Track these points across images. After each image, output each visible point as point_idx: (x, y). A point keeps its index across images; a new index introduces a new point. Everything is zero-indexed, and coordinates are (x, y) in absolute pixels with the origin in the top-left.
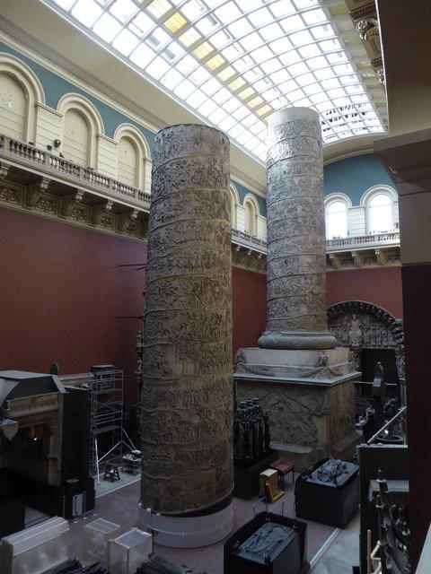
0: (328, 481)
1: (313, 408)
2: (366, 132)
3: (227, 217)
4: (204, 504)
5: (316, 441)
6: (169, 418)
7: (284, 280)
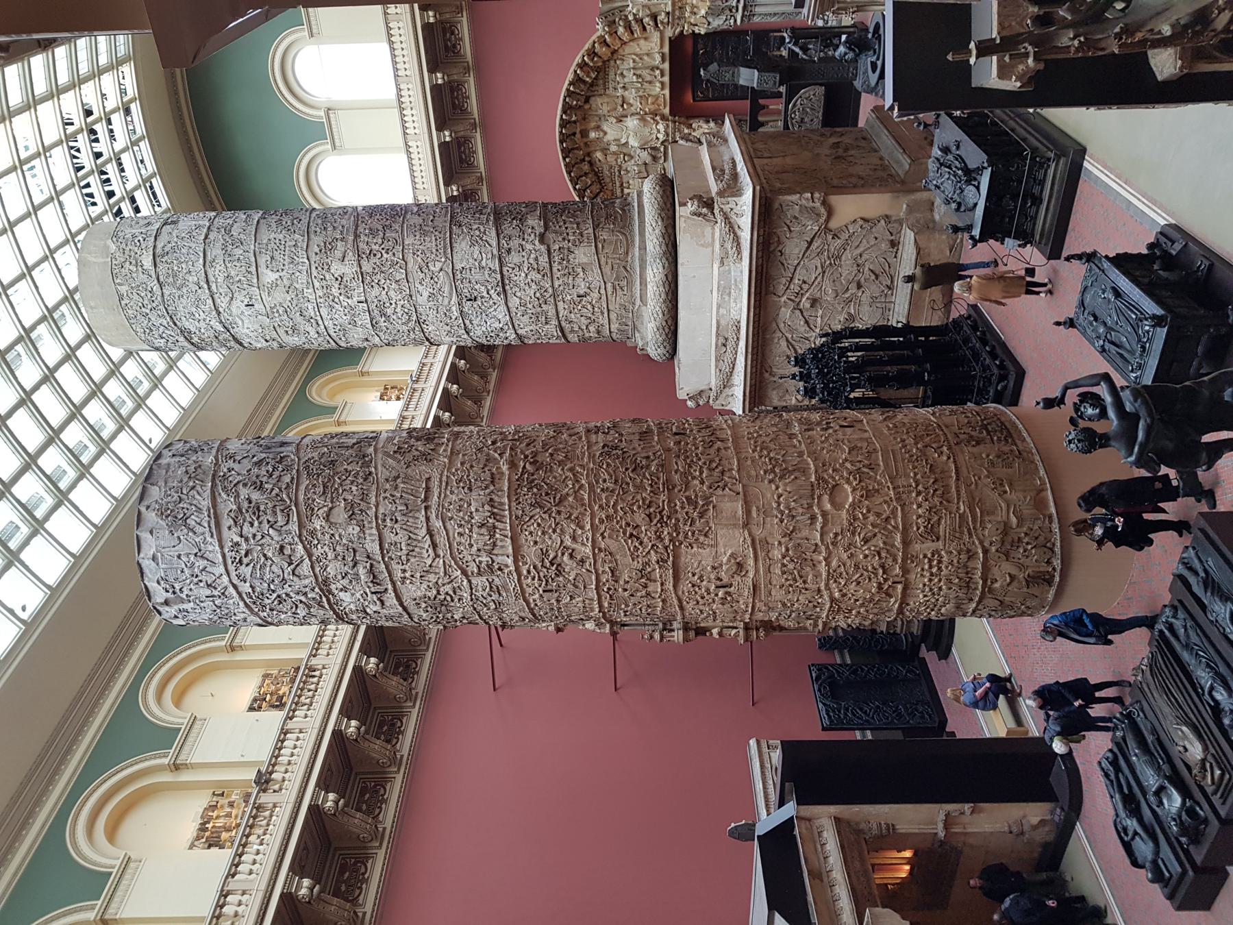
0: (978, 188)
1: (812, 227)
2: (135, 108)
3: (375, 437)
4: (1037, 469)
7: (514, 302)
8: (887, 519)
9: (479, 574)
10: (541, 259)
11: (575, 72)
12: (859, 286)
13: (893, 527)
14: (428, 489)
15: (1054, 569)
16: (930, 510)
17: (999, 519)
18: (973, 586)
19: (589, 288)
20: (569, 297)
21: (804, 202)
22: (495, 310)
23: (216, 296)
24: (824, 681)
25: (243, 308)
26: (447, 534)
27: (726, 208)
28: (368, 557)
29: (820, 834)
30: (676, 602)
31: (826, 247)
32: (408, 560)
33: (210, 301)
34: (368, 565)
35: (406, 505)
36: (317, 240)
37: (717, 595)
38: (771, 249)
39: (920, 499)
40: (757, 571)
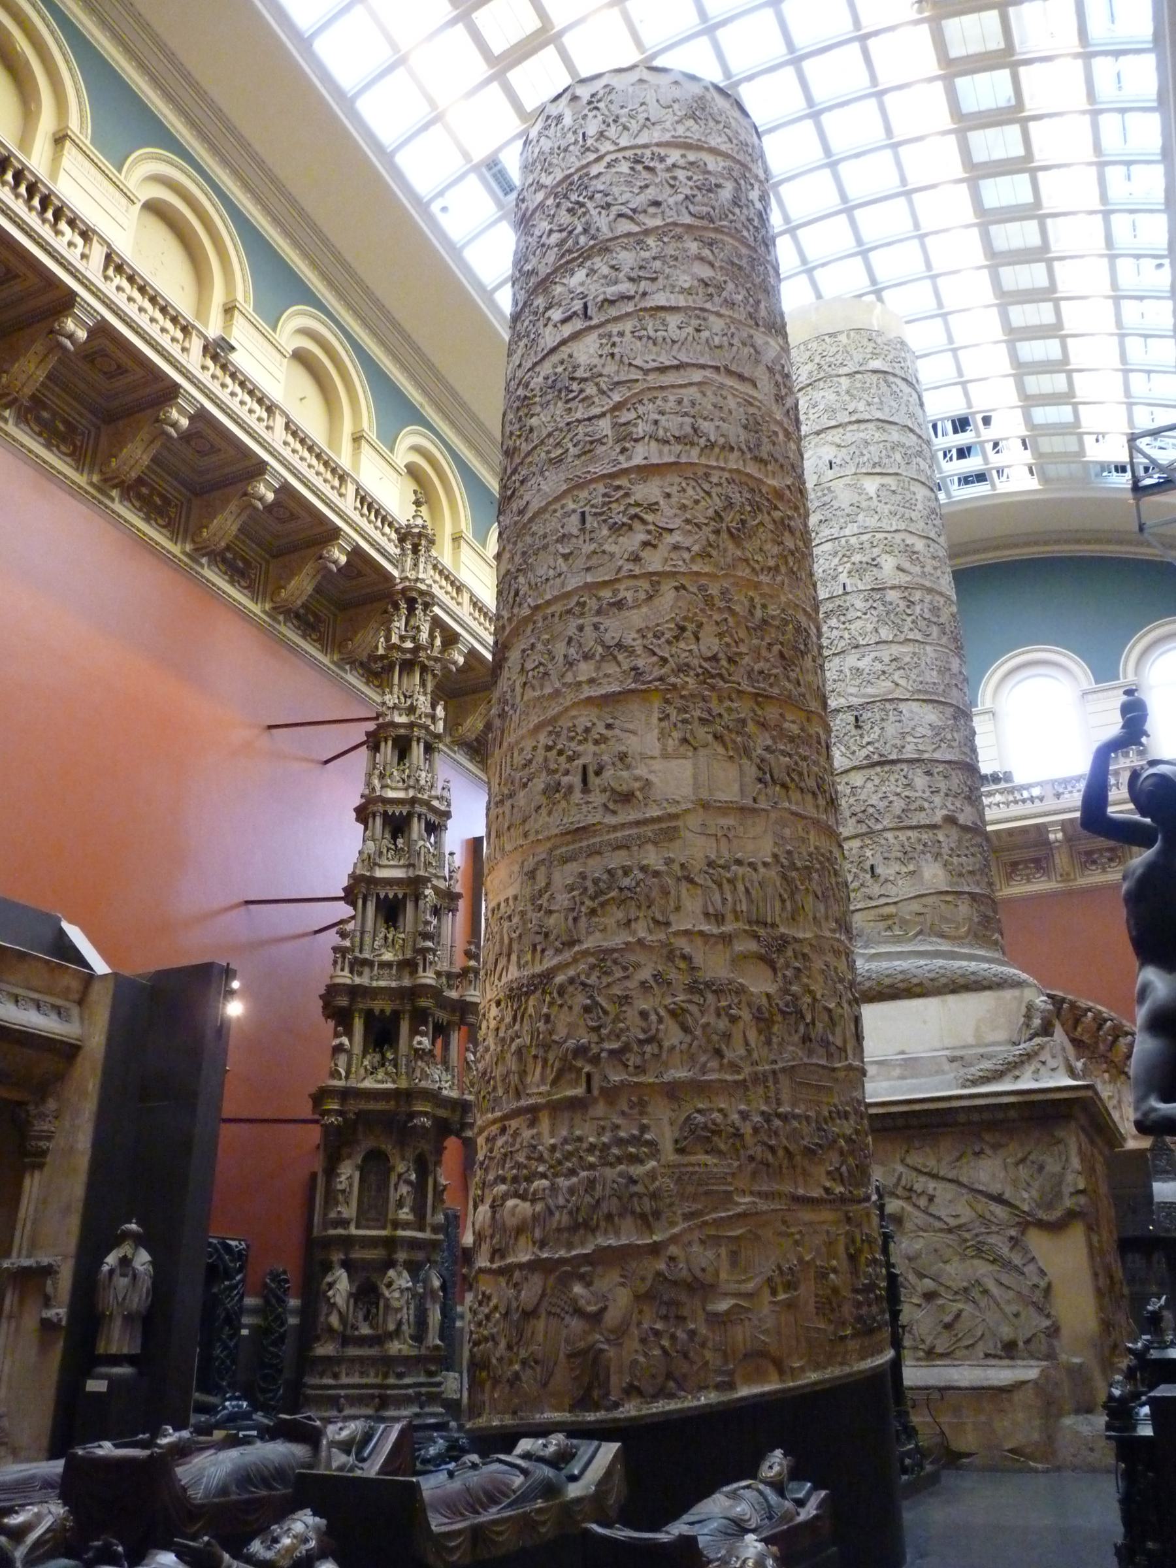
1: (1026, 1199)
4: (817, 1367)
5: (1054, 1331)
6: (645, 974)
8: (718, 1053)
9: (615, 425)
10: (923, 814)
11: (1089, 1010)
12: (930, 1296)
13: (704, 1065)
14: (741, 377)
15: (616, 1405)
16: (738, 1135)
17: (723, 1275)
18: (576, 1239)
19: (886, 881)
20: (869, 853)
21: (1070, 1177)
22: (843, 755)
23: (841, 430)
24: (220, 1257)
25: (826, 459)
26: (681, 386)
27: (1045, 1055)
28: (644, 294)
29: (58, 1010)
30: (551, 713)
31: (994, 1228)
32: (640, 338)
33: (833, 423)
34: (632, 293)
35: (720, 347)
36: (920, 545)
37: (567, 773)
38: (987, 1137)
39: (757, 1119)
40: (615, 828)
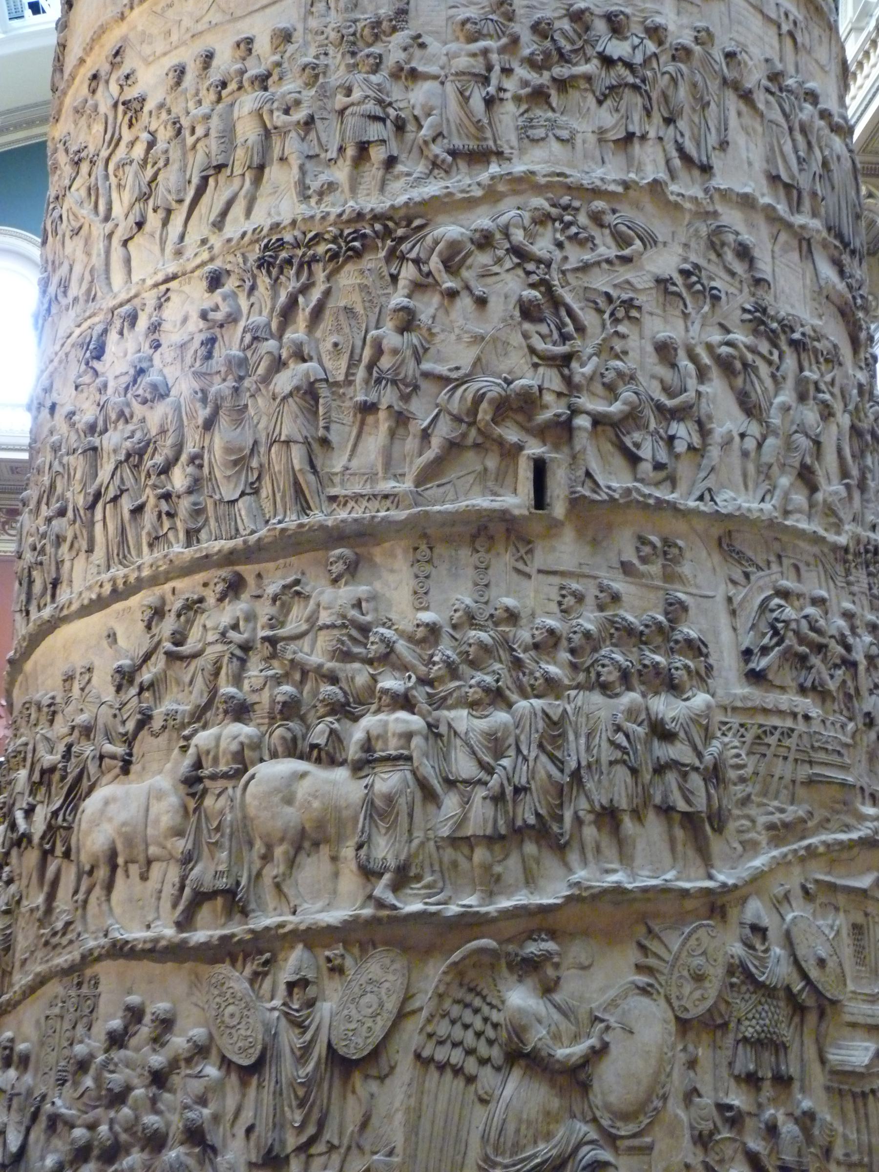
18: (511, 868)
